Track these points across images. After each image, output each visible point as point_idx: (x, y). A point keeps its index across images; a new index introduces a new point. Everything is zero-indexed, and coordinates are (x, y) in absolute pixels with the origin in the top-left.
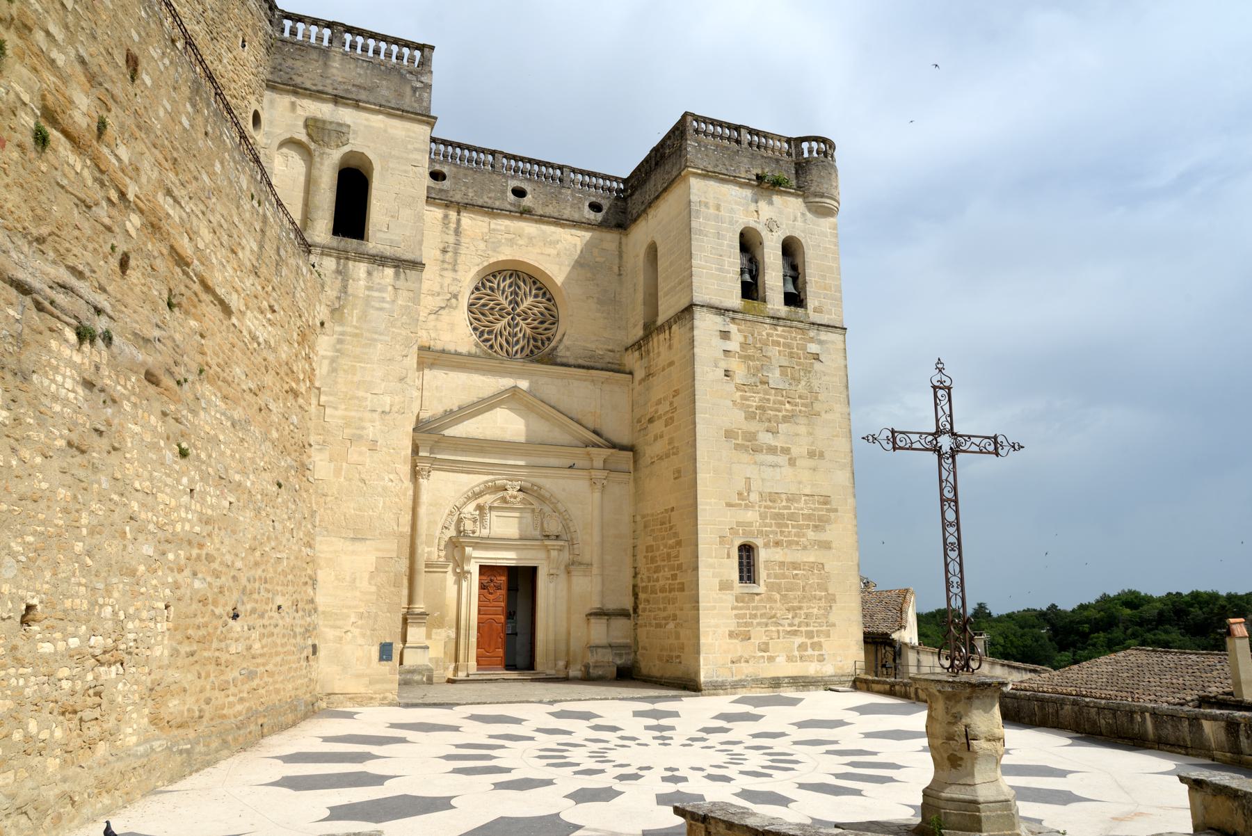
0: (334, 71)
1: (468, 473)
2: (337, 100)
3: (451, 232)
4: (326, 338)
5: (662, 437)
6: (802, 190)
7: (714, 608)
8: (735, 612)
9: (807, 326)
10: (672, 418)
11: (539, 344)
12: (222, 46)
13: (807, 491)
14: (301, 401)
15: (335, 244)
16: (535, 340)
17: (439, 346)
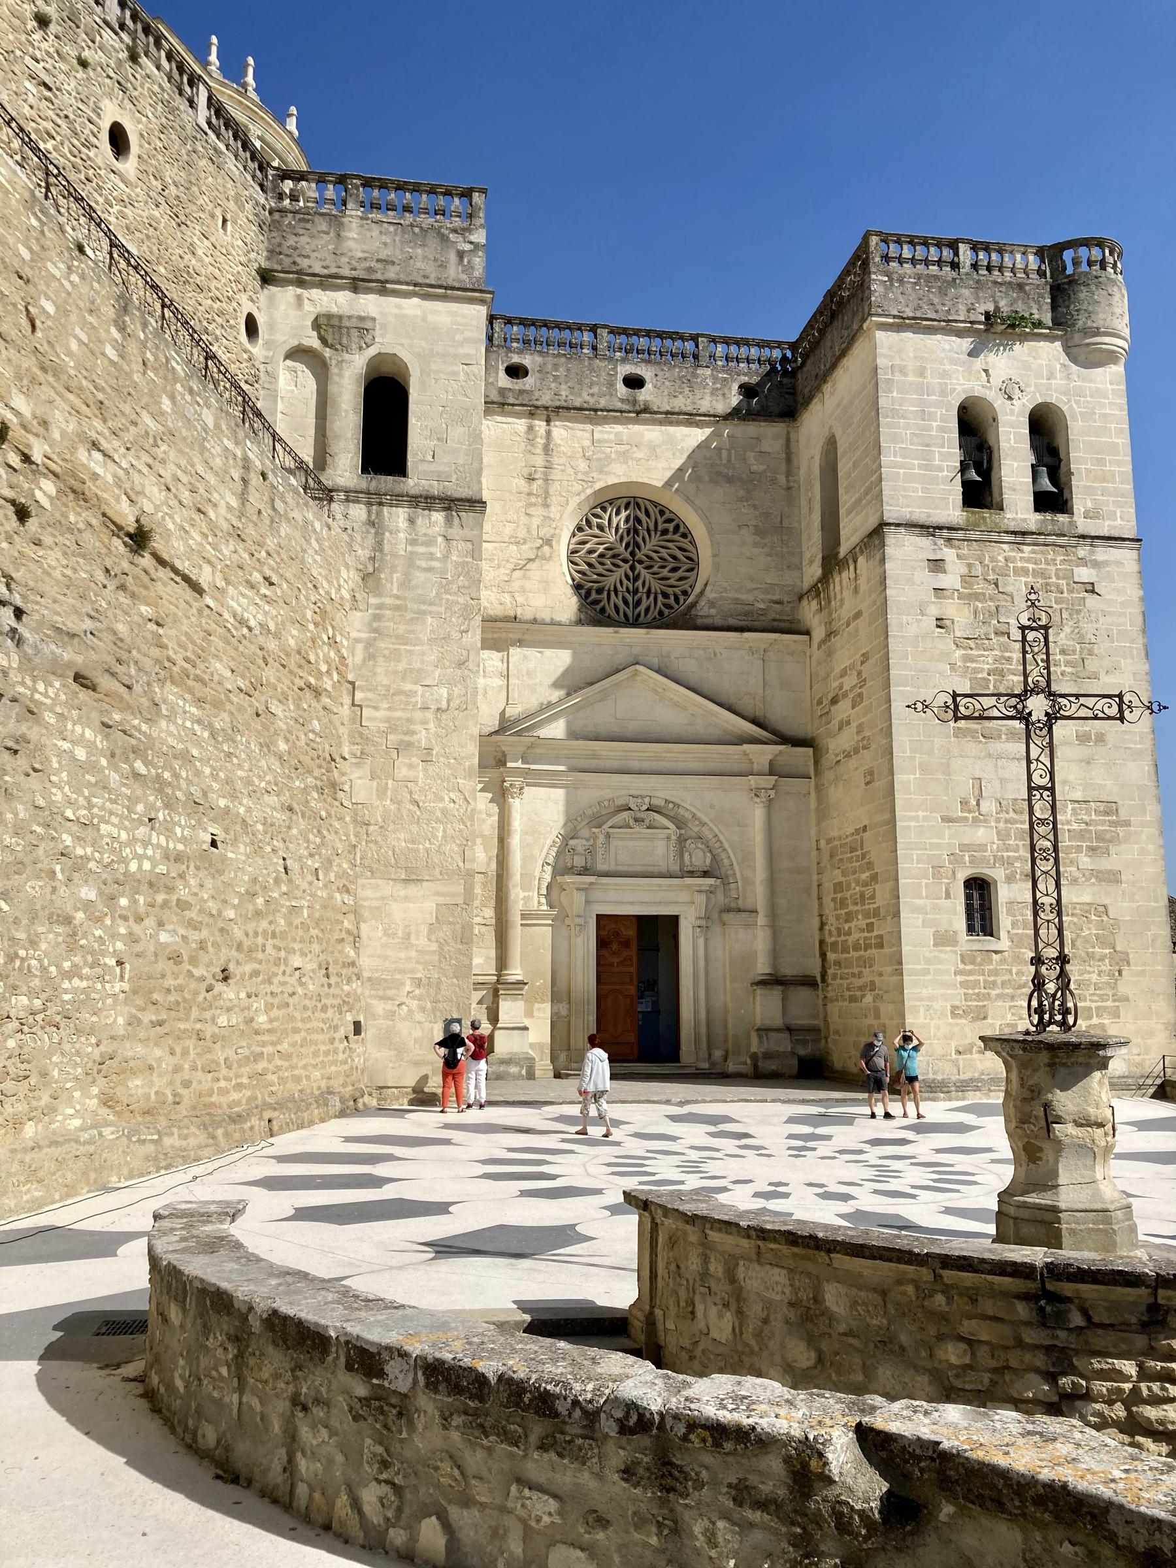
0: (351, 244)
2: (356, 285)
3: (539, 451)
4: (359, 614)
5: (848, 723)
7: (926, 972)
8: (959, 978)
9: (1073, 541)
10: (860, 695)
11: (672, 601)
12: (193, 234)
13: (1078, 795)
14: (326, 700)
15: (363, 485)
16: (665, 595)
17: (528, 614)
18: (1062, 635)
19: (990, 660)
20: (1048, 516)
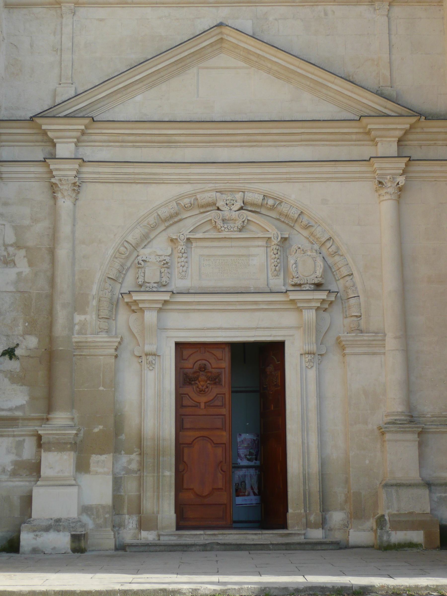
1: (146, 182)
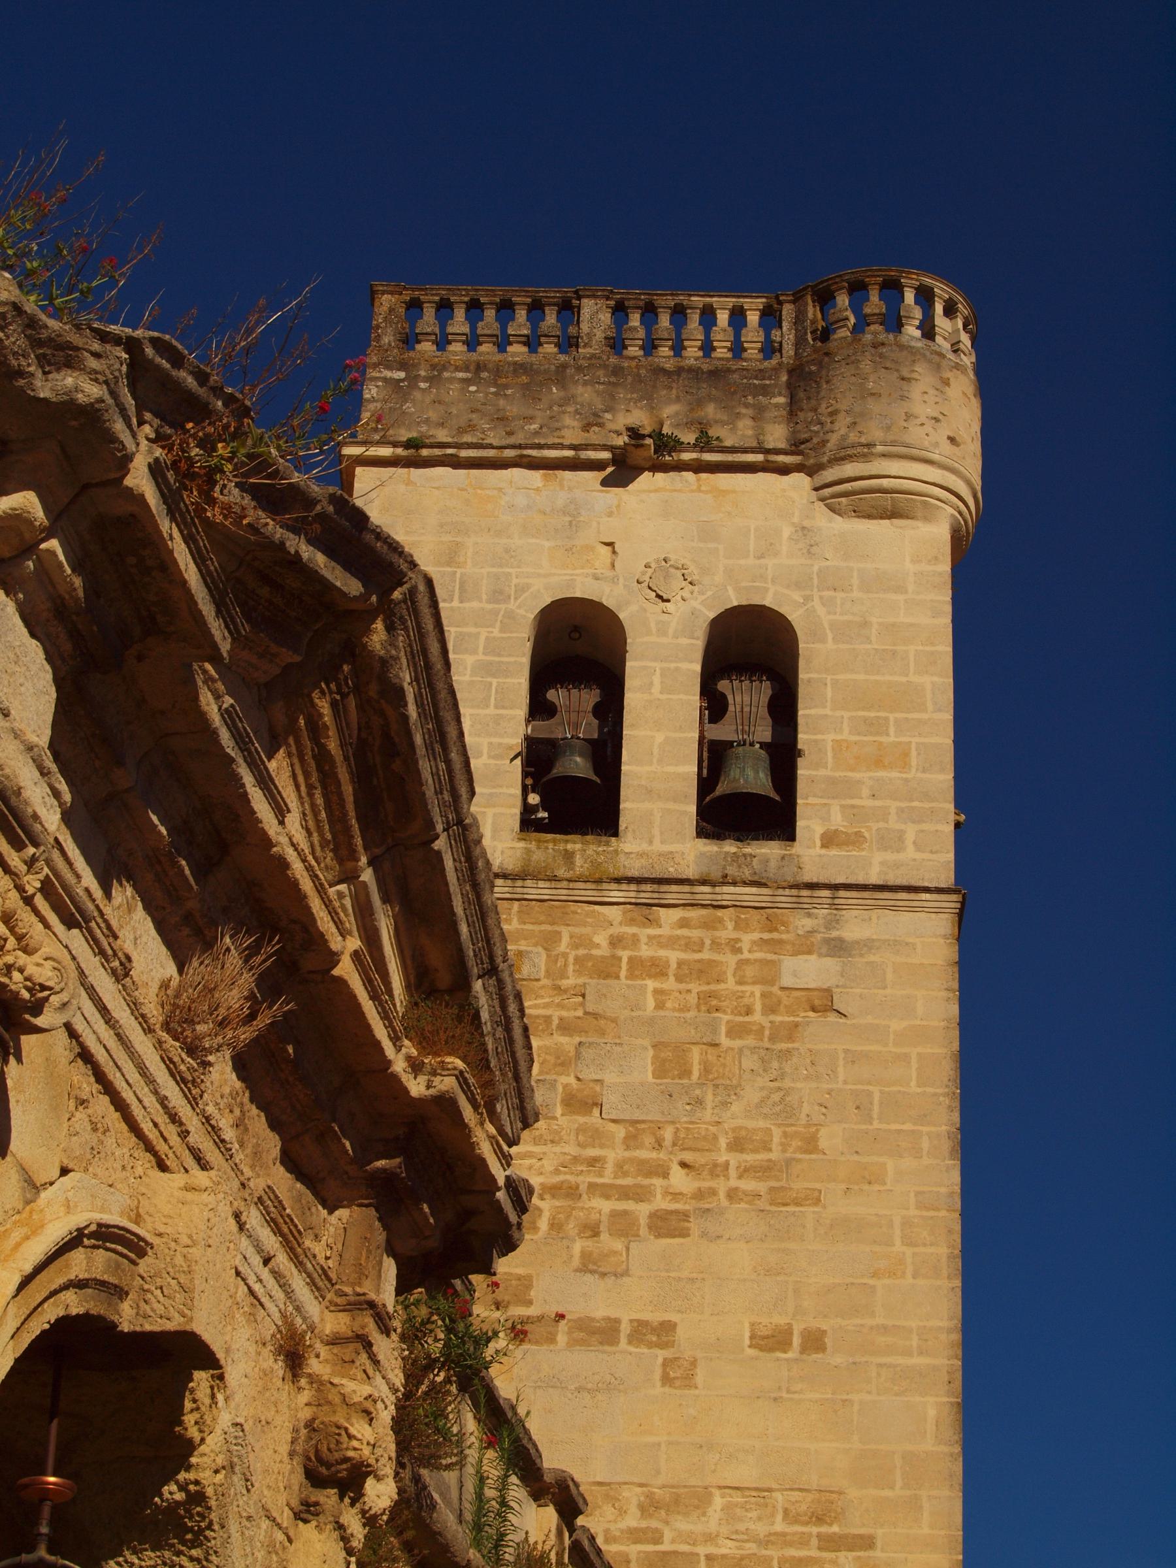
6: (804, 455)
9: (785, 897)
13: (745, 1473)
18: (736, 1108)
19: (548, 1165)
20: (730, 847)
